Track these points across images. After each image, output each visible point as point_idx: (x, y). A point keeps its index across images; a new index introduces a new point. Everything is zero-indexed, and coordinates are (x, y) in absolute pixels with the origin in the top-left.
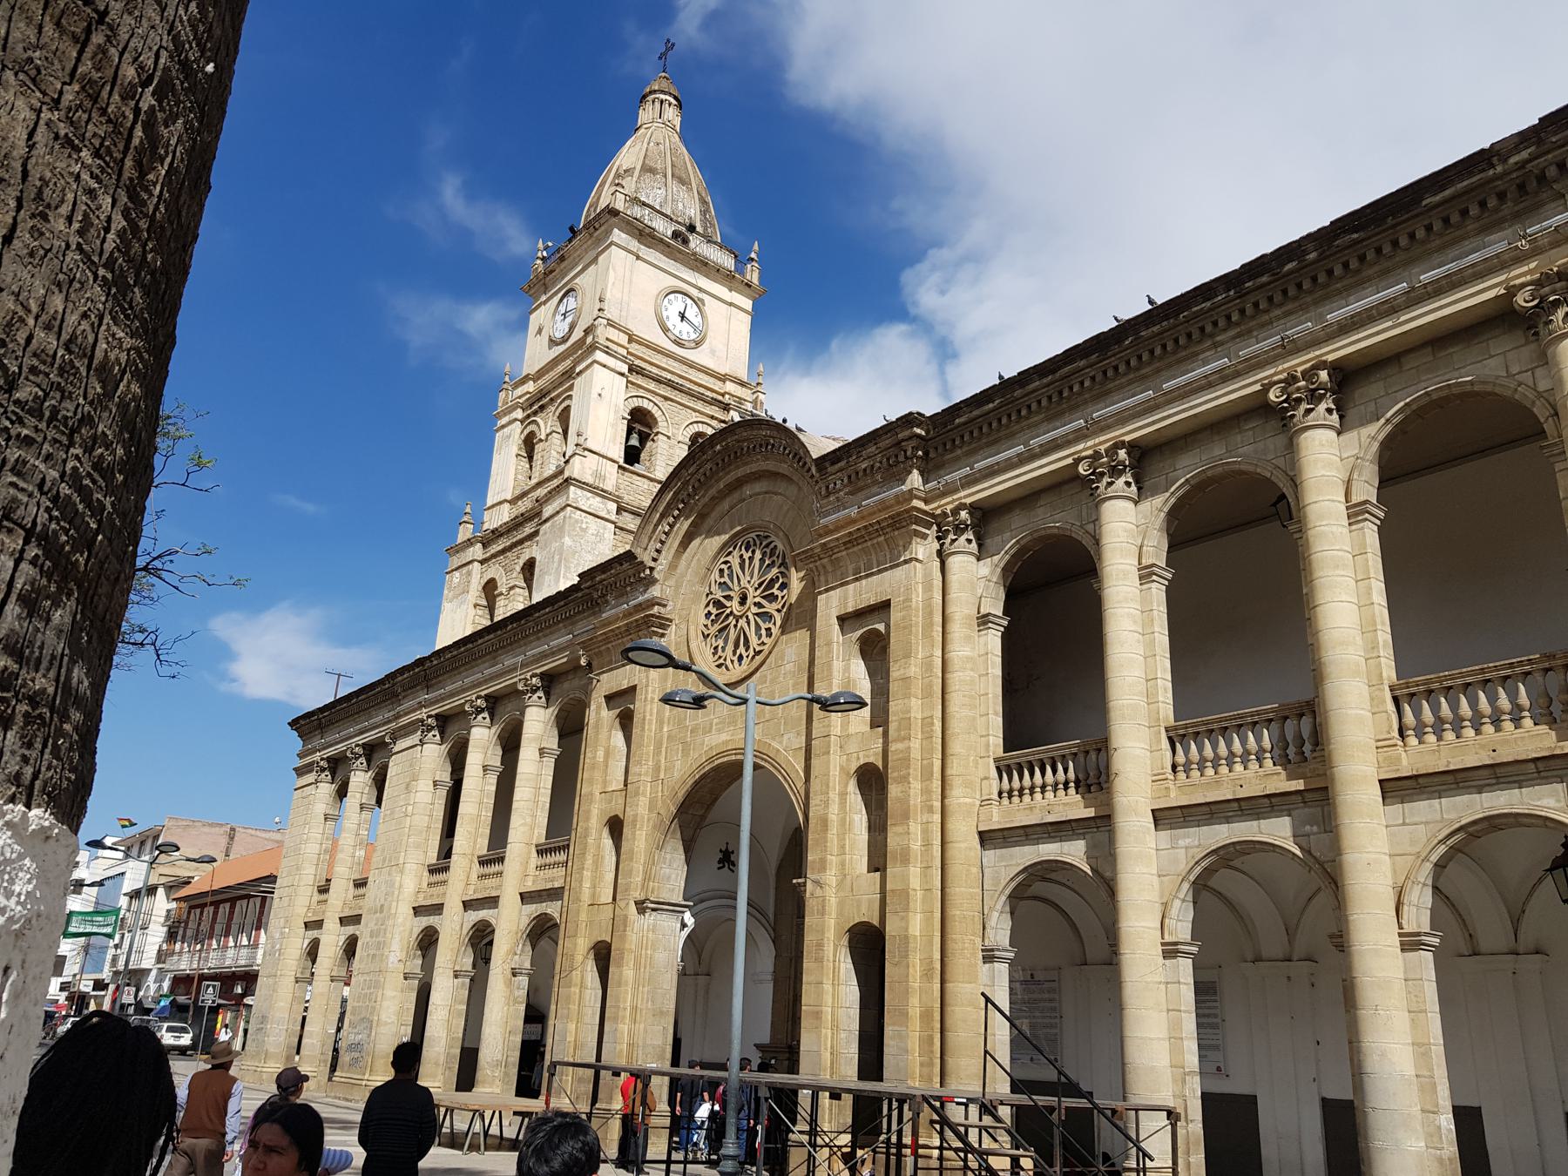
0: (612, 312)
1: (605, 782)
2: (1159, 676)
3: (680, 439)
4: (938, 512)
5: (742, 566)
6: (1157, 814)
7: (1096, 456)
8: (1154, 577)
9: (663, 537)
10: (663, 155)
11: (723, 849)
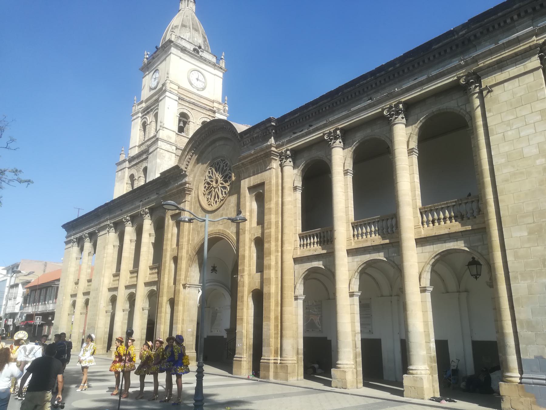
0: (172, 77)
2: (349, 206)
3: (198, 123)
4: (280, 152)
7: (330, 133)
8: (348, 173)
9: (189, 160)
11: (213, 266)
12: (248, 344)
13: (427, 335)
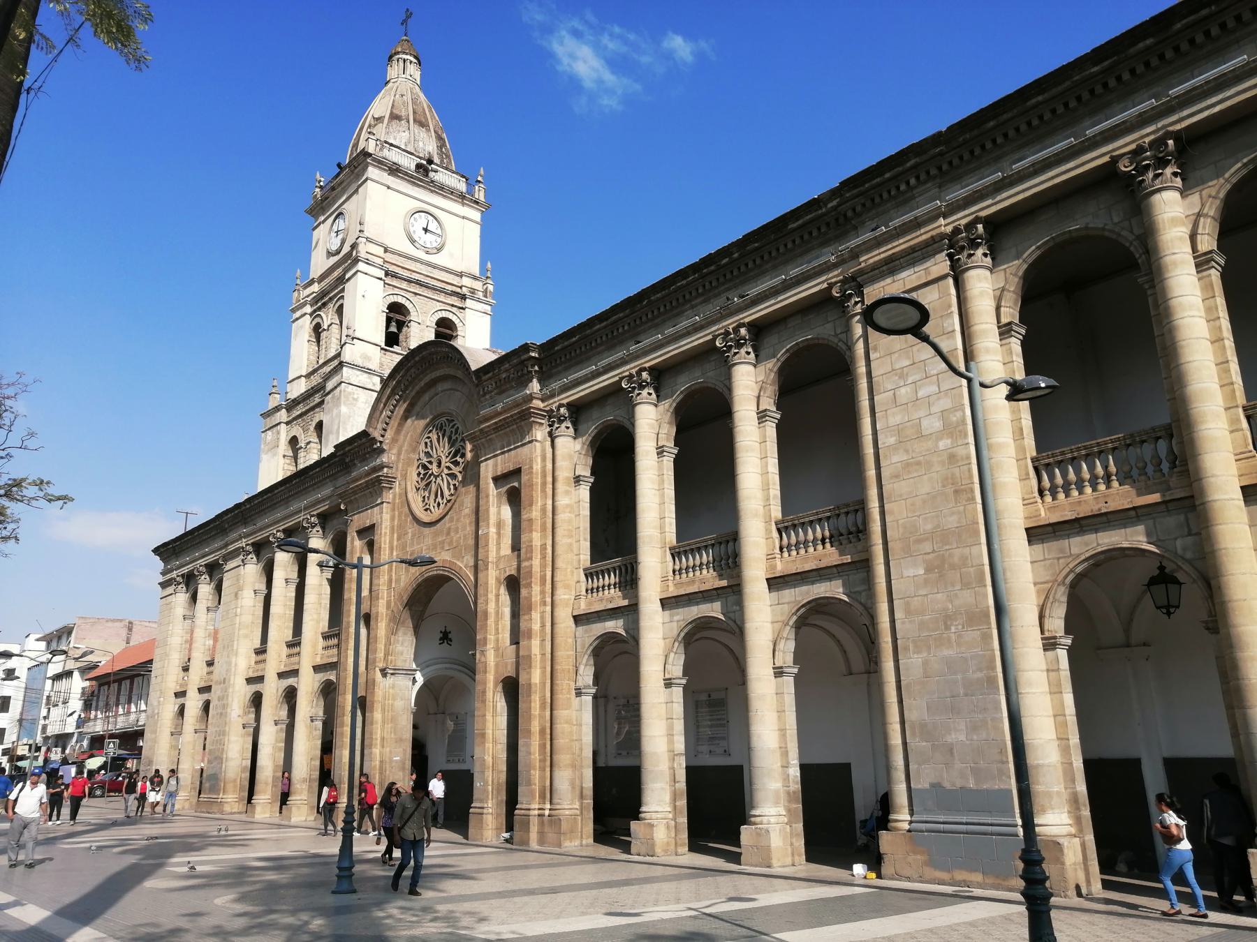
3: (428, 324)
4: (548, 409)
6: (663, 601)
7: (631, 376)
10: (405, 104)
12: (495, 781)
13: (785, 753)
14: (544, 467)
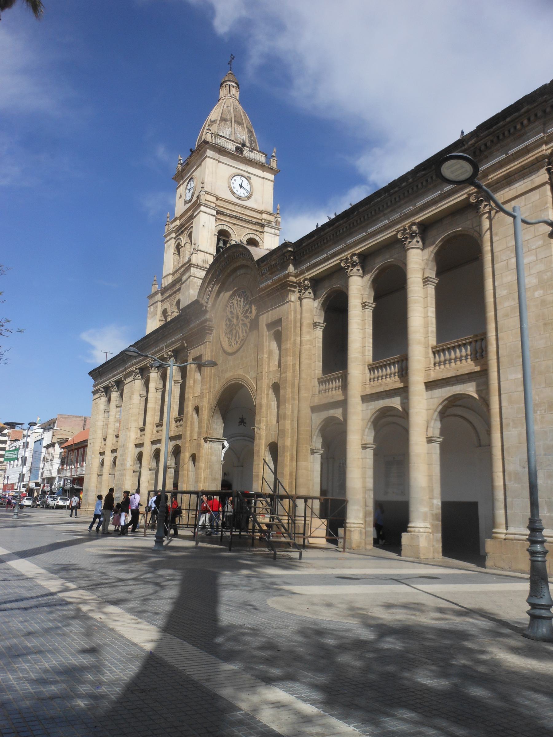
1: (194, 393)
4: (298, 282)
5: (237, 304)
7: (347, 259)
10: (230, 112)
14: (295, 317)
